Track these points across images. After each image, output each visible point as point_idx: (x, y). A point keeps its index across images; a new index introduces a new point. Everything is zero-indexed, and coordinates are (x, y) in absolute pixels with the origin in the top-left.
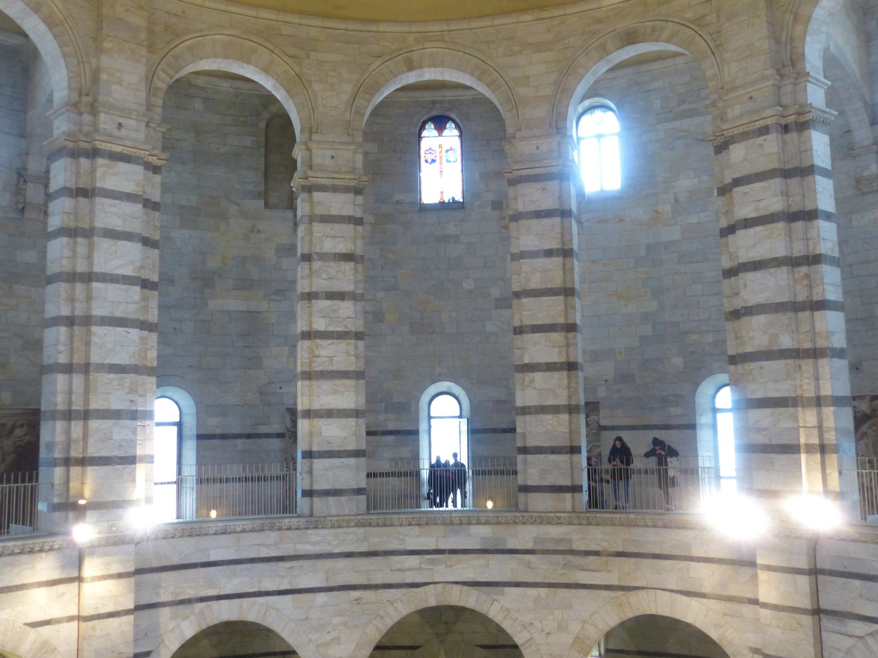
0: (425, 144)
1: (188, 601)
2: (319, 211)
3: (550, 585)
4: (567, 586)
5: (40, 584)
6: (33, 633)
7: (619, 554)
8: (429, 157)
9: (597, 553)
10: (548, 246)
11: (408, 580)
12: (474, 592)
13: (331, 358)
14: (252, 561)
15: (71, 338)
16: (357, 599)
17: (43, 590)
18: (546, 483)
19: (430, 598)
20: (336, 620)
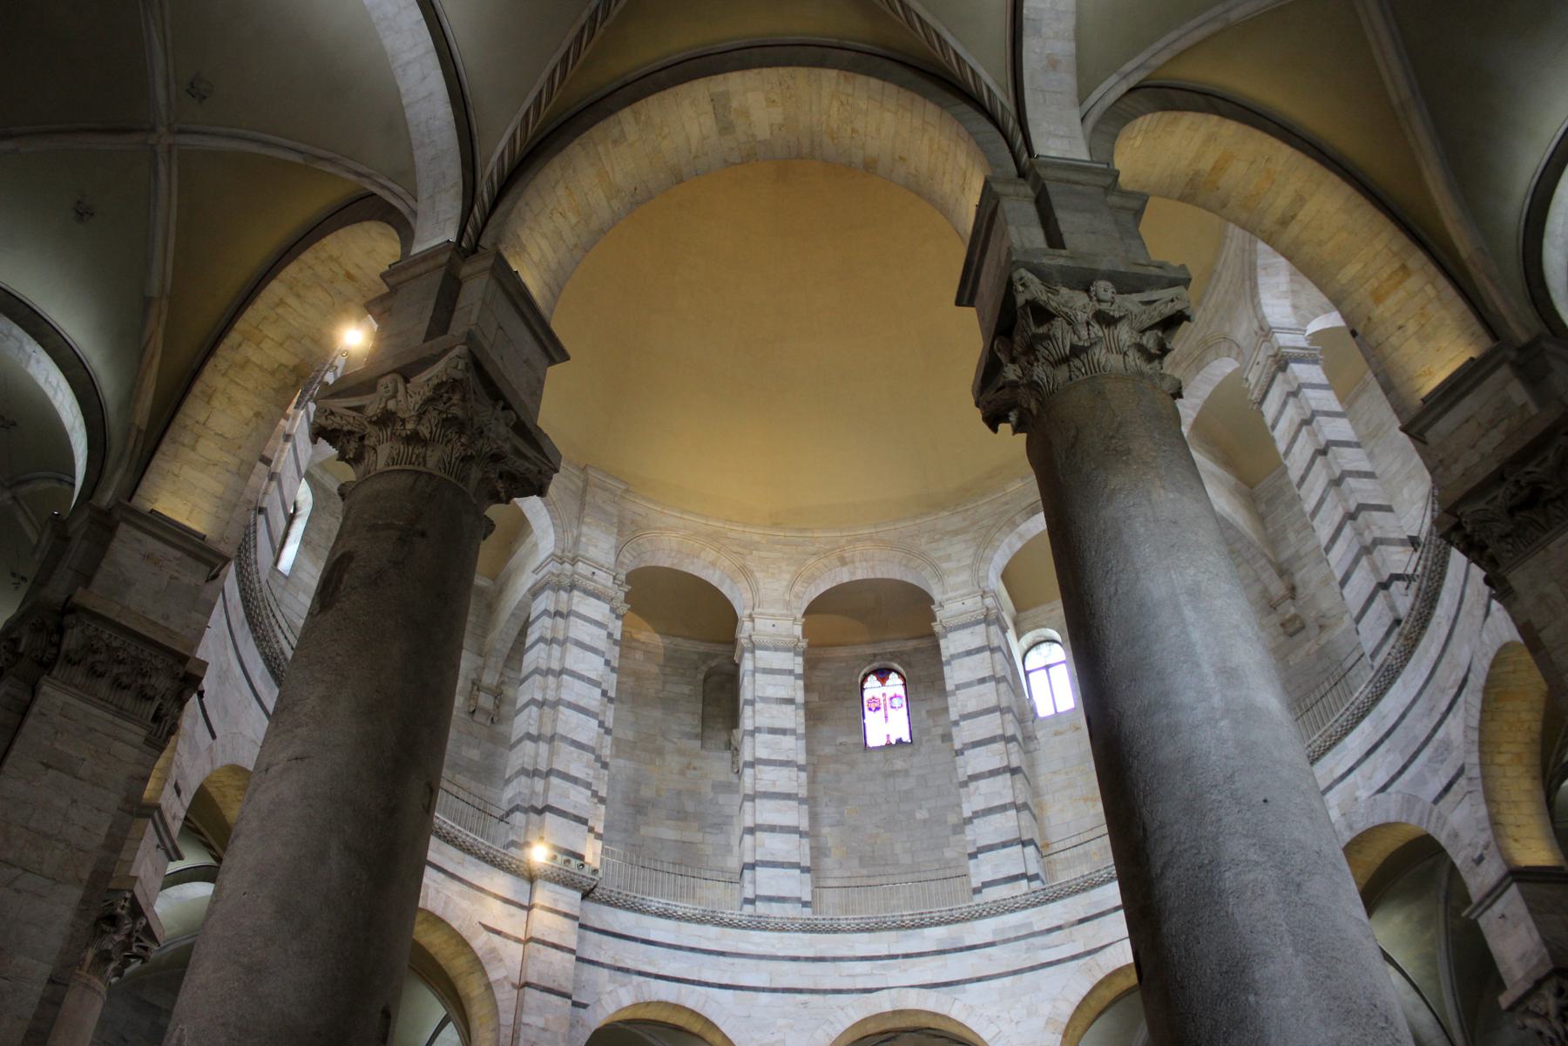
0: (867, 695)
1: (627, 971)
2: (760, 664)
3: (1015, 973)
4: (1032, 968)
5: (496, 897)
6: (485, 935)
7: (1081, 921)
8: (873, 706)
9: (1059, 928)
10: (980, 676)
11: (860, 986)
12: (933, 993)
13: (774, 783)
14: (692, 950)
15: (541, 717)
16: (805, 1004)
17: (499, 903)
18: (1001, 876)
19: (884, 1003)
20: (781, 1022)
